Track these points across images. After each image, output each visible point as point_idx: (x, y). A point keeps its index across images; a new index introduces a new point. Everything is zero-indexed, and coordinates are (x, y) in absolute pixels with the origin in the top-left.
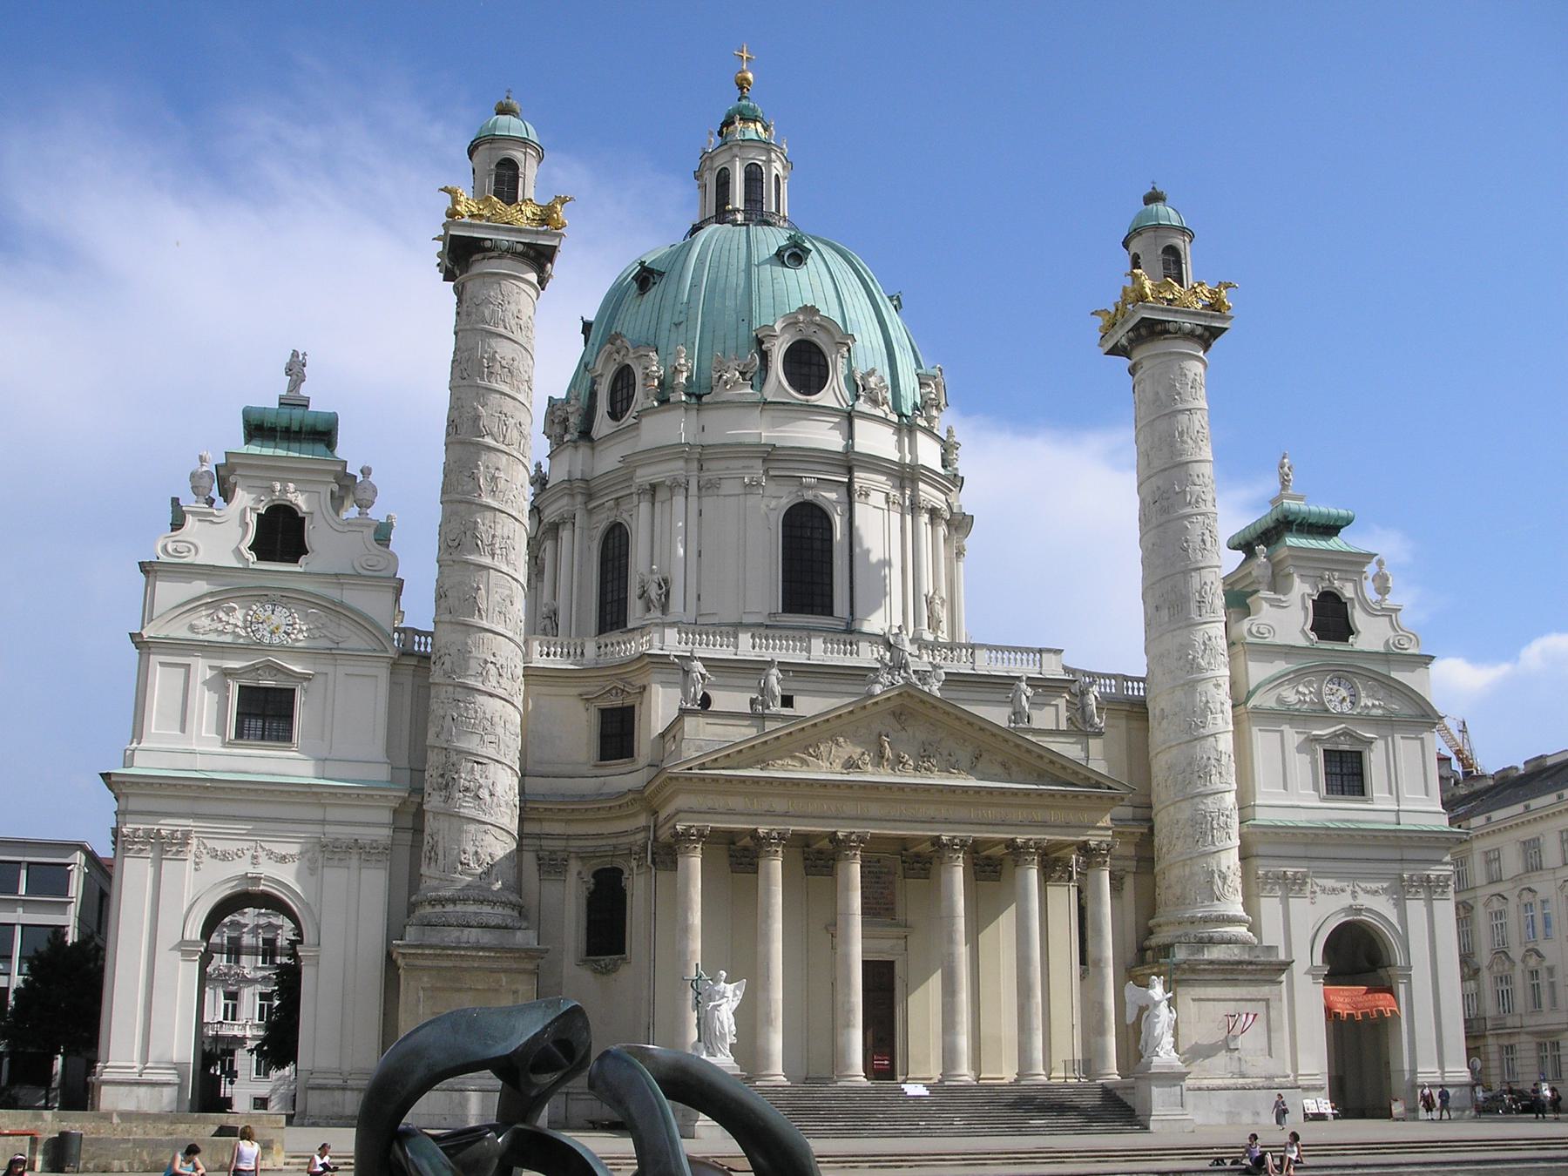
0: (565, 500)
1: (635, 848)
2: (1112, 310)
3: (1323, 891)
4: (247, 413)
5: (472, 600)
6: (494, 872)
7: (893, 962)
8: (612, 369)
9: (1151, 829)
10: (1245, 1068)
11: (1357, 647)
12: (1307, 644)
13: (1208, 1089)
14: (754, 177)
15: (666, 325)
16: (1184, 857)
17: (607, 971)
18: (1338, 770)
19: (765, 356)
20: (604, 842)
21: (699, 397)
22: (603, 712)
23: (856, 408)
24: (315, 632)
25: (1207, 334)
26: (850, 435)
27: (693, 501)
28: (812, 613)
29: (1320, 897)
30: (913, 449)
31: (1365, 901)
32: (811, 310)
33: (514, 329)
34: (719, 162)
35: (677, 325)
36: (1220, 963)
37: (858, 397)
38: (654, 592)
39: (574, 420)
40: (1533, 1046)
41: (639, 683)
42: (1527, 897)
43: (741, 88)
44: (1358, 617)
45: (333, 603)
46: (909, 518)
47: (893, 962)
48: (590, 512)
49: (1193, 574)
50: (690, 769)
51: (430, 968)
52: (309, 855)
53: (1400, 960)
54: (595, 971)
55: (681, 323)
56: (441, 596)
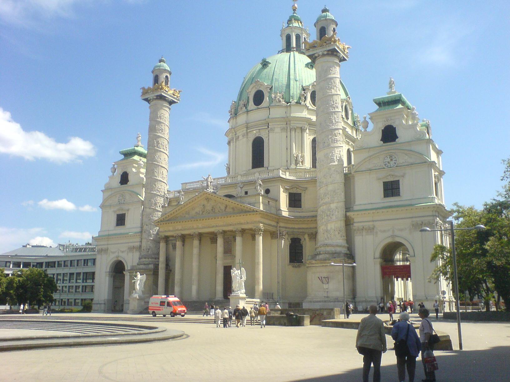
4: (120, 152)
10: (329, 296)
11: (399, 142)
12: (379, 145)
13: (314, 302)
14: (289, 38)
18: (391, 188)
19: (248, 98)
21: (237, 114)
25: (330, 52)
26: (270, 114)
31: (397, 233)
36: (321, 260)
43: (293, 10)
44: (398, 133)
46: (289, 133)
50: (159, 222)
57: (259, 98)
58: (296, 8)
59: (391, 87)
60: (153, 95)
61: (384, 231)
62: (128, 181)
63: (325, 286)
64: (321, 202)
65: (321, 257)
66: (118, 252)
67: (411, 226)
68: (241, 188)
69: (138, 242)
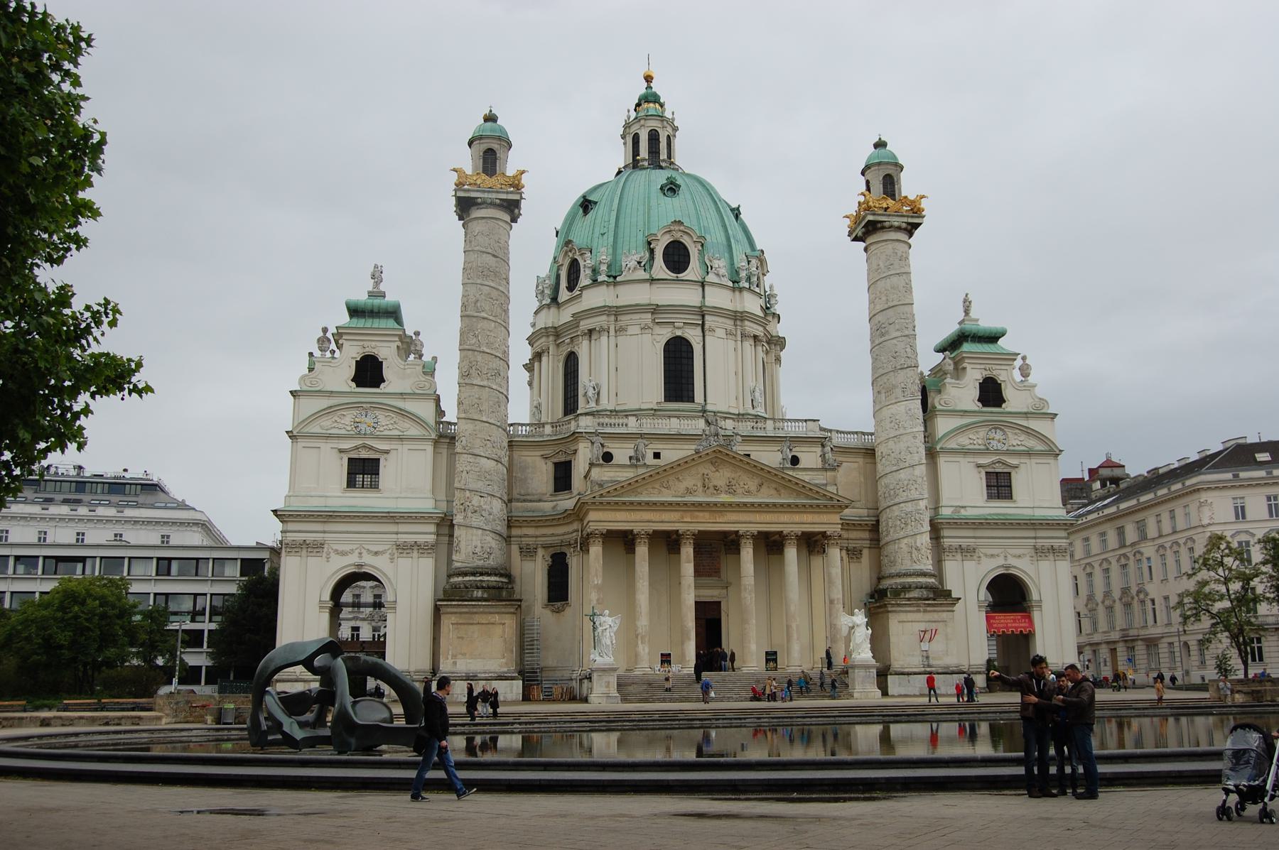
0: (543, 339)
1: (572, 542)
2: (855, 214)
3: (986, 555)
5: (476, 405)
6: (493, 555)
7: (720, 602)
8: (567, 262)
9: (878, 521)
10: (932, 662)
11: (1009, 410)
12: (977, 409)
13: (909, 674)
14: (654, 137)
15: (597, 234)
16: (895, 538)
17: (558, 611)
19: (652, 251)
20: (557, 538)
21: (615, 277)
22: (556, 464)
23: (706, 280)
24: (390, 426)
25: (909, 227)
26: (704, 297)
27: (612, 339)
28: (682, 401)
29: (983, 558)
30: (742, 299)
31: (1012, 561)
32: (680, 223)
33: (496, 249)
34: (634, 129)
35: (603, 235)
36: (915, 599)
37: (708, 273)
38: (591, 392)
39: (547, 292)
40: (1144, 647)
41: (573, 448)
42: (1138, 556)
43: (647, 81)
44: (1008, 392)
45: (400, 409)
47: (720, 602)
48: (558, 345)
49: (899, 371)
51: (456, 613)
52: (390, 551)
53: (1035, 596)
54: (553, 611)
55: (603, 235)
56: (460, 403)
57: (677, 257)
58: (652, 78)
59: (967, 312)
60: (494, 196)
61: (992, 556)
62: (384, 381)
63: (925, 646)
64: (903, 496)
65: (912, 594)
66: (360, 554)
67: (1033, 551)
68: (791, 450)
69: (430, 533)
